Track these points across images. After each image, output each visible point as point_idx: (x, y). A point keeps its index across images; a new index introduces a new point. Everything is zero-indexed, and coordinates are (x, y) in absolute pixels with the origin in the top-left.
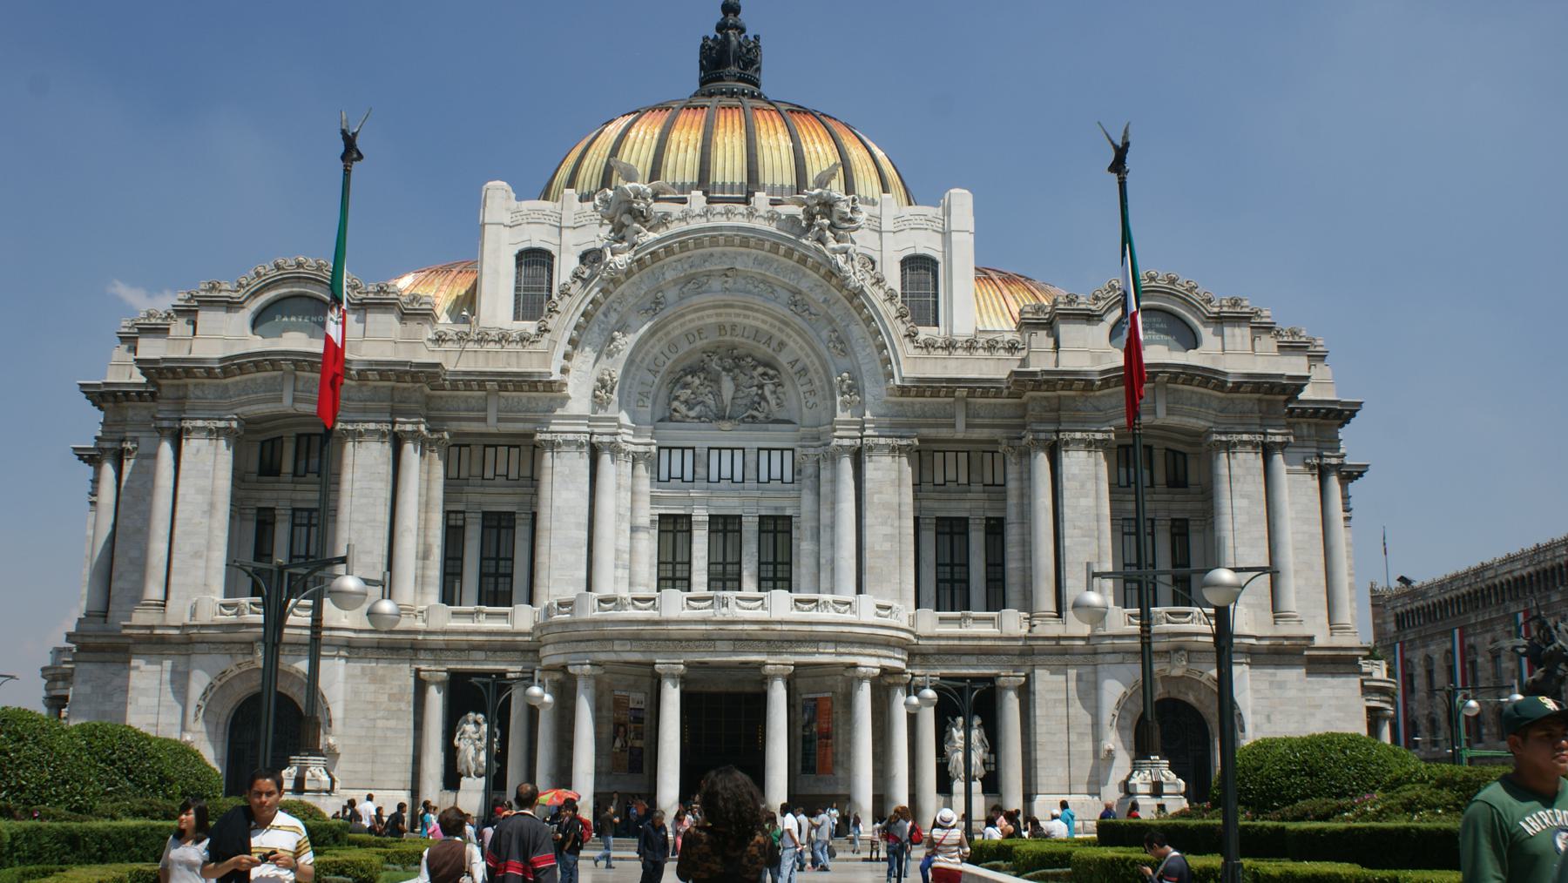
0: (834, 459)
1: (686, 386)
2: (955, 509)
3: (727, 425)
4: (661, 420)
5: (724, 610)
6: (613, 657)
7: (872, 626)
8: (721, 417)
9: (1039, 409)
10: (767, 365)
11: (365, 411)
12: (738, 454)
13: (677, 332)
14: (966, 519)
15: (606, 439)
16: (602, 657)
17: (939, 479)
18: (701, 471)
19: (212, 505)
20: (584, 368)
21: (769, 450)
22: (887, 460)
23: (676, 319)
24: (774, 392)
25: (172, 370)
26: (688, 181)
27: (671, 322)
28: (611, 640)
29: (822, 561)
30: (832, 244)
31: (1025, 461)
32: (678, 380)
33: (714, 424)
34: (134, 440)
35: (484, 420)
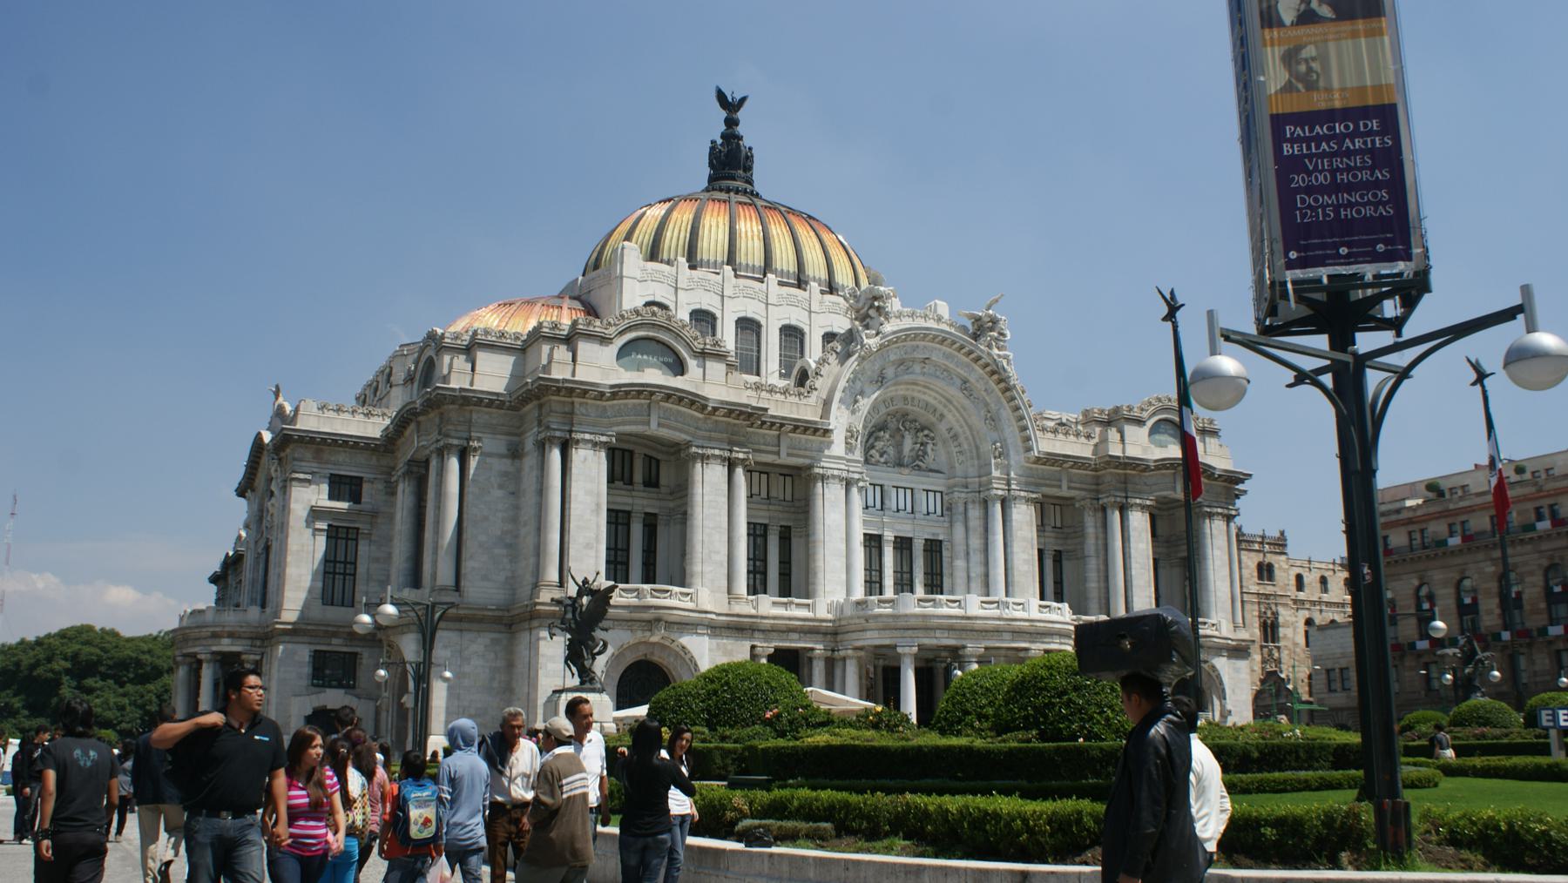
0: (985, 504)
1: (877, 439)
3: (906, 471)
6: (934, 642)
8: (899, 464)
9: (1113, 482)
11: (710, 439)
16: (926, 641)
19: (598, 505)
22: (1024, 507)
25: (571, 391)
26: (757, 264)
28: (934, 629)
29: (973, 575)
30: (995, 351)
31: (1100, 515)
34: (479, 439)
35: (778, 453)
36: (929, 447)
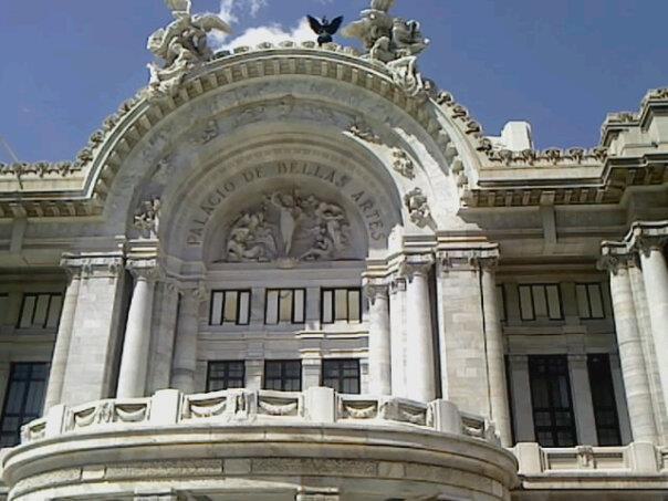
2: (548, 346)
3: (287, 262)
4: (216, 262)
5: (242, 414)
7: (457, 440)
10: (330, 203)
12: (299, 295)
13: (234, 171)
14: (566, 355)
15: (142, 264)
17: (528, 314)
18: (257, 313)
20: (124, 192)
21: (333, 290)
23: (232, 154)
24: (340, 229)
27: (227, 157)
32: (236, 222)
33: (273, 263)
36: (332, 225)
